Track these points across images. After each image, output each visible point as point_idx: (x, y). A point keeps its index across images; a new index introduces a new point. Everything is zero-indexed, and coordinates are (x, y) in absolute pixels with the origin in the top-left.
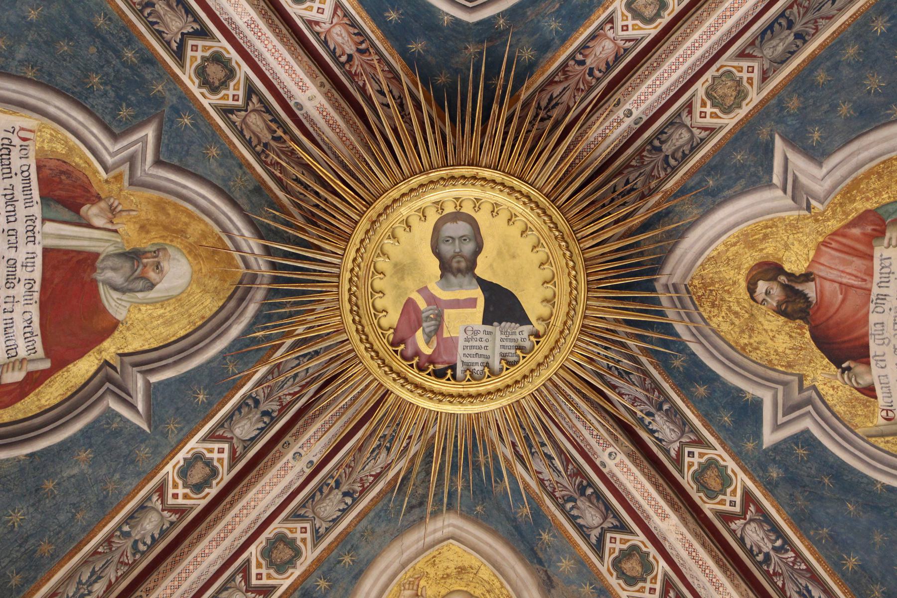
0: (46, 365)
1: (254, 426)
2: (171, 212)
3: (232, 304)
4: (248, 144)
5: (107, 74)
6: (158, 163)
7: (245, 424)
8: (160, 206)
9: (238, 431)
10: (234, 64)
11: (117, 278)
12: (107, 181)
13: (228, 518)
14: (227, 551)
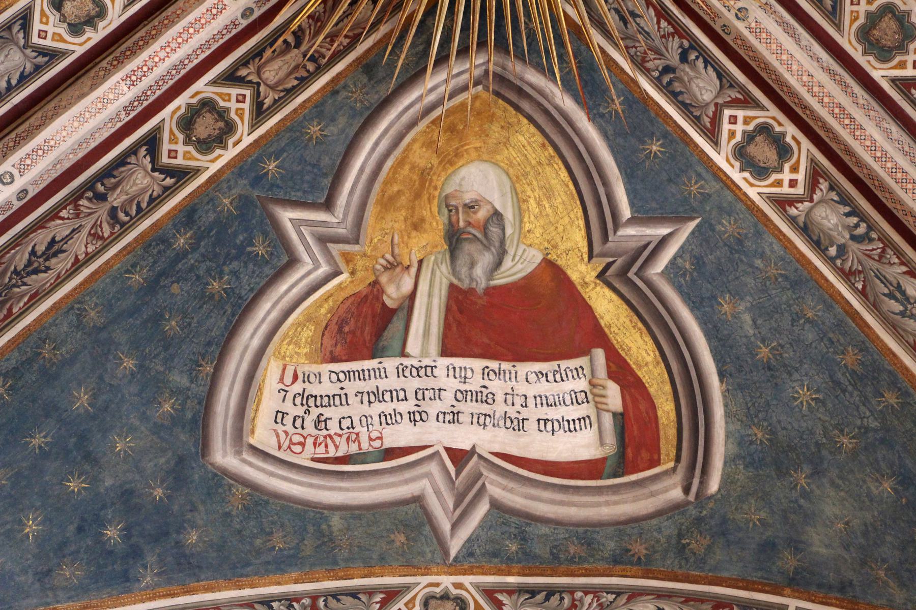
0: (599, 354)
1: (700, 73)
2: (396, 188)
3: (526, 105)
4: (304, 82)
5: (208, 271)
6: (328, 205)
7: (698, 86)
8: (388, 203)
9: (707, 97)
10: (194, 101)
11: (485, 260)
12: (353, 273)
13: (823, 113)
14: (872, 113)
